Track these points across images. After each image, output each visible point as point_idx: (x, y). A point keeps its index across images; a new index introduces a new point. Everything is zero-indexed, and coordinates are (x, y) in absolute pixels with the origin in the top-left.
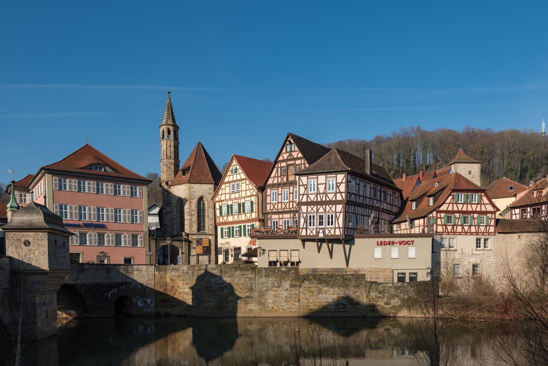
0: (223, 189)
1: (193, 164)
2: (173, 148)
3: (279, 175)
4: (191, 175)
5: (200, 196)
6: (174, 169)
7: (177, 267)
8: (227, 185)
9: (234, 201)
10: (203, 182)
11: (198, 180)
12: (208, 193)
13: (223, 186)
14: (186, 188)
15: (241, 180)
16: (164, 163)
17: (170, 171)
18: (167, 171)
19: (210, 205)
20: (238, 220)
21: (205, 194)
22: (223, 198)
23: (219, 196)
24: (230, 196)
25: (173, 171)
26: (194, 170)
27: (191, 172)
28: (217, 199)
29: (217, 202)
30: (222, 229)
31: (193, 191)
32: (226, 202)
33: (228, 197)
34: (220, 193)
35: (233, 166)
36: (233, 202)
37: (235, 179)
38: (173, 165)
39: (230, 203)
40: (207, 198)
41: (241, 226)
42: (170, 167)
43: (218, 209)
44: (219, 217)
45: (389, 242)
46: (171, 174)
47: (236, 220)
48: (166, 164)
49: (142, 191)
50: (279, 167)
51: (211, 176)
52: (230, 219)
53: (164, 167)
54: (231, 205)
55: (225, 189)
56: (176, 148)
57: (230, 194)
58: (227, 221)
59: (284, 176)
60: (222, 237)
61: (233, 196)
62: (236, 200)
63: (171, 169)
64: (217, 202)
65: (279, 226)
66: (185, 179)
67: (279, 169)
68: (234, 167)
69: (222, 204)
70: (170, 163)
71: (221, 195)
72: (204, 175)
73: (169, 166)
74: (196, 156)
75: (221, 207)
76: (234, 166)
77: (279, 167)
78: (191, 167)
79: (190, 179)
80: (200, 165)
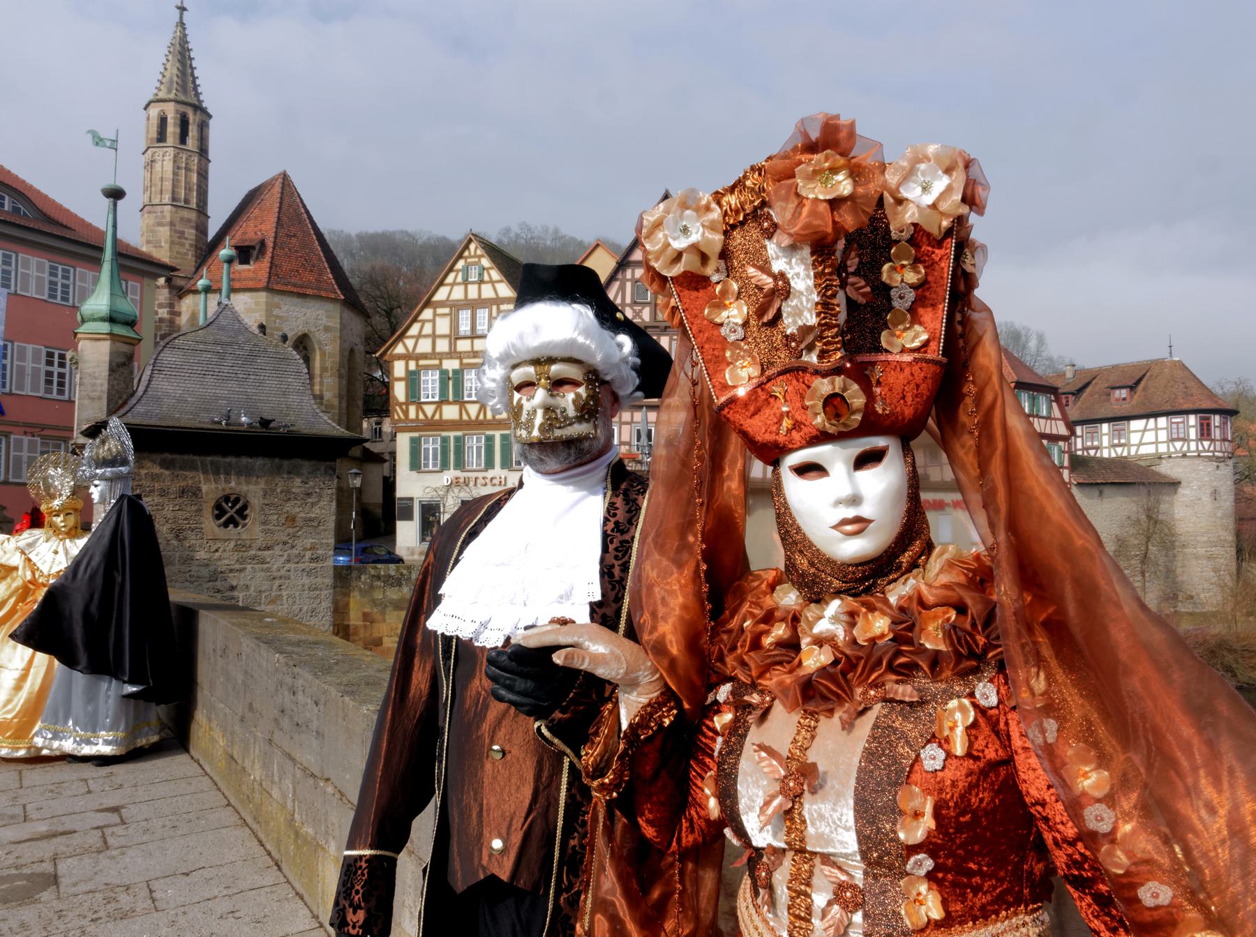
0: (424, 322)
1: (273, 235)
2: (195, 175)
3: (628, 300)
4: (271, 268)
5: (300, 333)
6: (196, 241)
7: (393, 573)
8: (440, 311)
9: (465, 361)
10: (309, 292)
11: (295, 285)
12: (321, 327)
13: (427, 314)
14: (257, 304)
15: (498, 301)
16: (164, 217)
17: (183, 245)
18: (172, 243)
19: (328, 364)
20: (481, 417)
21: (313, 330)
22: (424, 346)
23: (410, 343)
24: (452, 345)
25: (191, 245)
26: (278, 252)
27: (272, 258)
28: (400, 349)
29: (400, 357)
30: (415, 444)
31: (278, 317)
32: (436, 362)
33: (443, 346)
34: (414, 330)
35: (466, 258)
36: (461, 364)
37: (473, 292)
38: (191, 227)
39: (451, 365)
40: (320, 343)
41: (490, 439)
42: (183, 233)
43: (400, 379)
44: (407, 404)
45: (935, 501)
46: (186, 254)
47: (473, 417)
48: (168, 219)
49: (138, 298)
50: (628, 280)
51: (330, 276)
52: (451, 412)
53: (161, 229)
54: (458, 374)
55: (433, 321)
56: (203, 175)
57: (454, 336)
58: (437, 417)
59: (644, 304)
60: (415, 465)
61: (463, 346)
62: (475, 357)
63: (187, 239)
64: (400, 357)
65: (621, 443)
66: (251, 275)
67: (629, 285)
68: (469, 260)
69: (417, 365)
70: (182, 219)
71: (419, 336)
72: (311, 271)
73: (179, 228)
74: (279, 213)
75: (413, 380)
76: (470, 257)
77: (628, 280)
78: (270, 244)
79: (269, 278)
80: (294, 240)
